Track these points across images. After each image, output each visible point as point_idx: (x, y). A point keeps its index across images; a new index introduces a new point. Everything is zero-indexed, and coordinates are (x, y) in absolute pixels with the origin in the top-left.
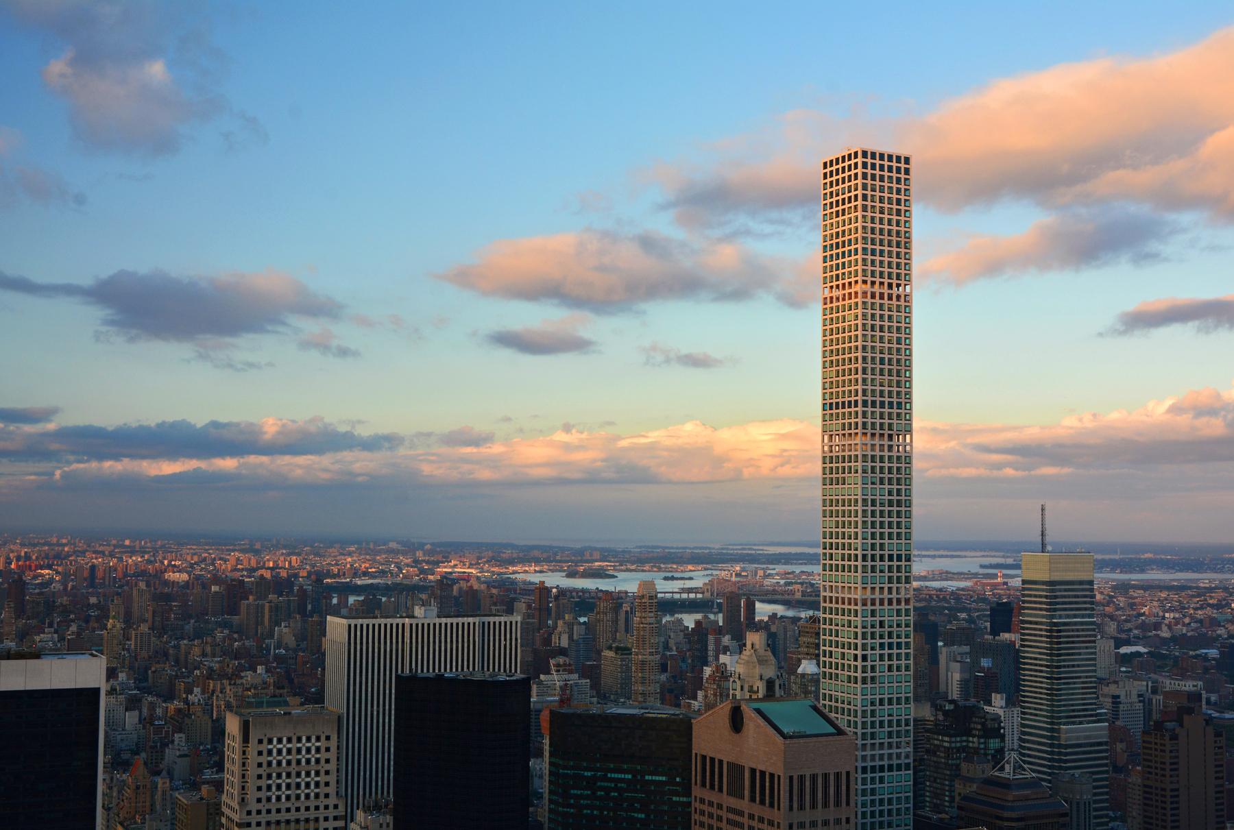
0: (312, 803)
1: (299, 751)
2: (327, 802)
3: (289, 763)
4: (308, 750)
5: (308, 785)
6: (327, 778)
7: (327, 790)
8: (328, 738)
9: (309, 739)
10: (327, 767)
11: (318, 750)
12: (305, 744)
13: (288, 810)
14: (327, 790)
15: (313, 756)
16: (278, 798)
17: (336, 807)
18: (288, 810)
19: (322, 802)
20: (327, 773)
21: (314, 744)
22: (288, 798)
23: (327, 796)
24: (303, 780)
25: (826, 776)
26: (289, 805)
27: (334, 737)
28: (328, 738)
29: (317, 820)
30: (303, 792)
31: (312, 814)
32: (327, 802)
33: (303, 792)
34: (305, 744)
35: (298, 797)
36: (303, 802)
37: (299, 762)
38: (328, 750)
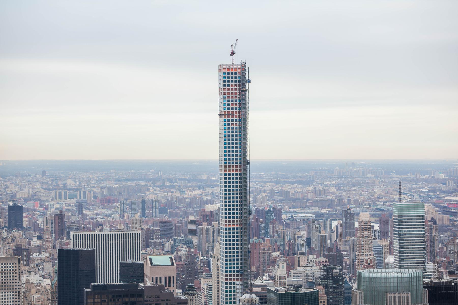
0: (12, 281)
1: (8, 267)
2: (16, 281)
3: (5, 270)
4: (10, 267)
5: (10, 276)
6: (16, 275)
7: (16, 278)
8: (16, 264)
9: (10, 264)
10: (16, 272)
11: (13, 267)
12: (9, 265)
13: (5, 283)
14: (16, 278)
15: (12, 269)
16: (10, 279)
17: (19, 282)
18: (5, 283)
19: (14, 281)
20: (16, 273)
21: (12, 265)
22: (5, 280)
23: (16, 279)
24: (9, 275)
25: (165, 278)
26: (5, 281)
27: (18, 263)
28: (16, 264)
29: (13, 286)
30: (9, 278)
31: (12, 284)
32: (16, 281)
33: (9, 278)
34: (9, 265)
35: (8, 280)
36: (9, 281)
37: (8, 270)
38: (16, 267)
